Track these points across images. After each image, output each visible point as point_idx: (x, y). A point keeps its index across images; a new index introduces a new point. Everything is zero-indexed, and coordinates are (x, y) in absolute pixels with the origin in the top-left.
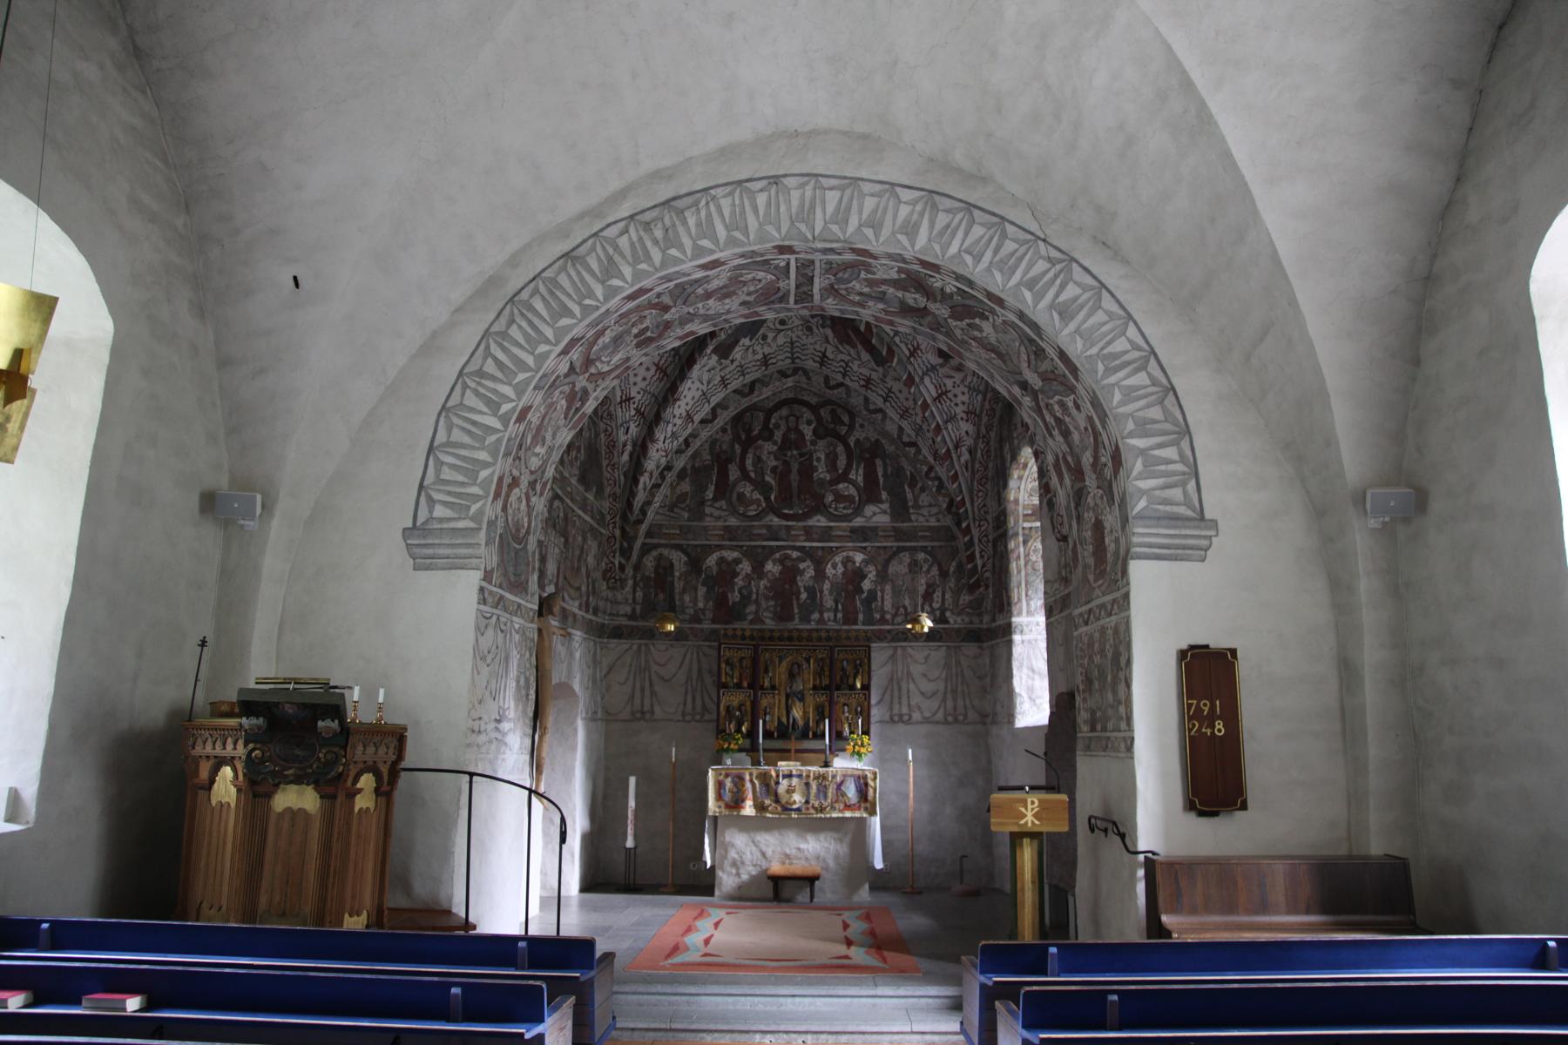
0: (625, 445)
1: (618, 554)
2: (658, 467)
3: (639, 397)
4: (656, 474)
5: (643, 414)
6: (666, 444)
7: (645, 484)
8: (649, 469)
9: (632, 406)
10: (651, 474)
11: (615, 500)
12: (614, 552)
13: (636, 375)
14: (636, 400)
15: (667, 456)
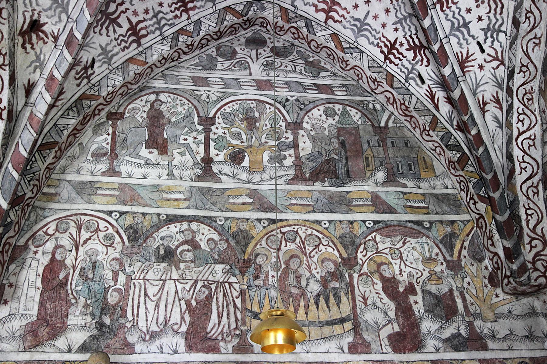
0: (432, 97)
1: (497, 236)
2: (500, 86)
3: (400, 34)
4: (502, 96)
5: (422, 46)
6: (488, 50)
7: (496, 119)
8: (488, 97)
9: (402, 50)
10: (497, 101)
11: (455, 168)
12: (491, 238)
13: (375, 17)
14: (401, 39)
15: (502, 63)
